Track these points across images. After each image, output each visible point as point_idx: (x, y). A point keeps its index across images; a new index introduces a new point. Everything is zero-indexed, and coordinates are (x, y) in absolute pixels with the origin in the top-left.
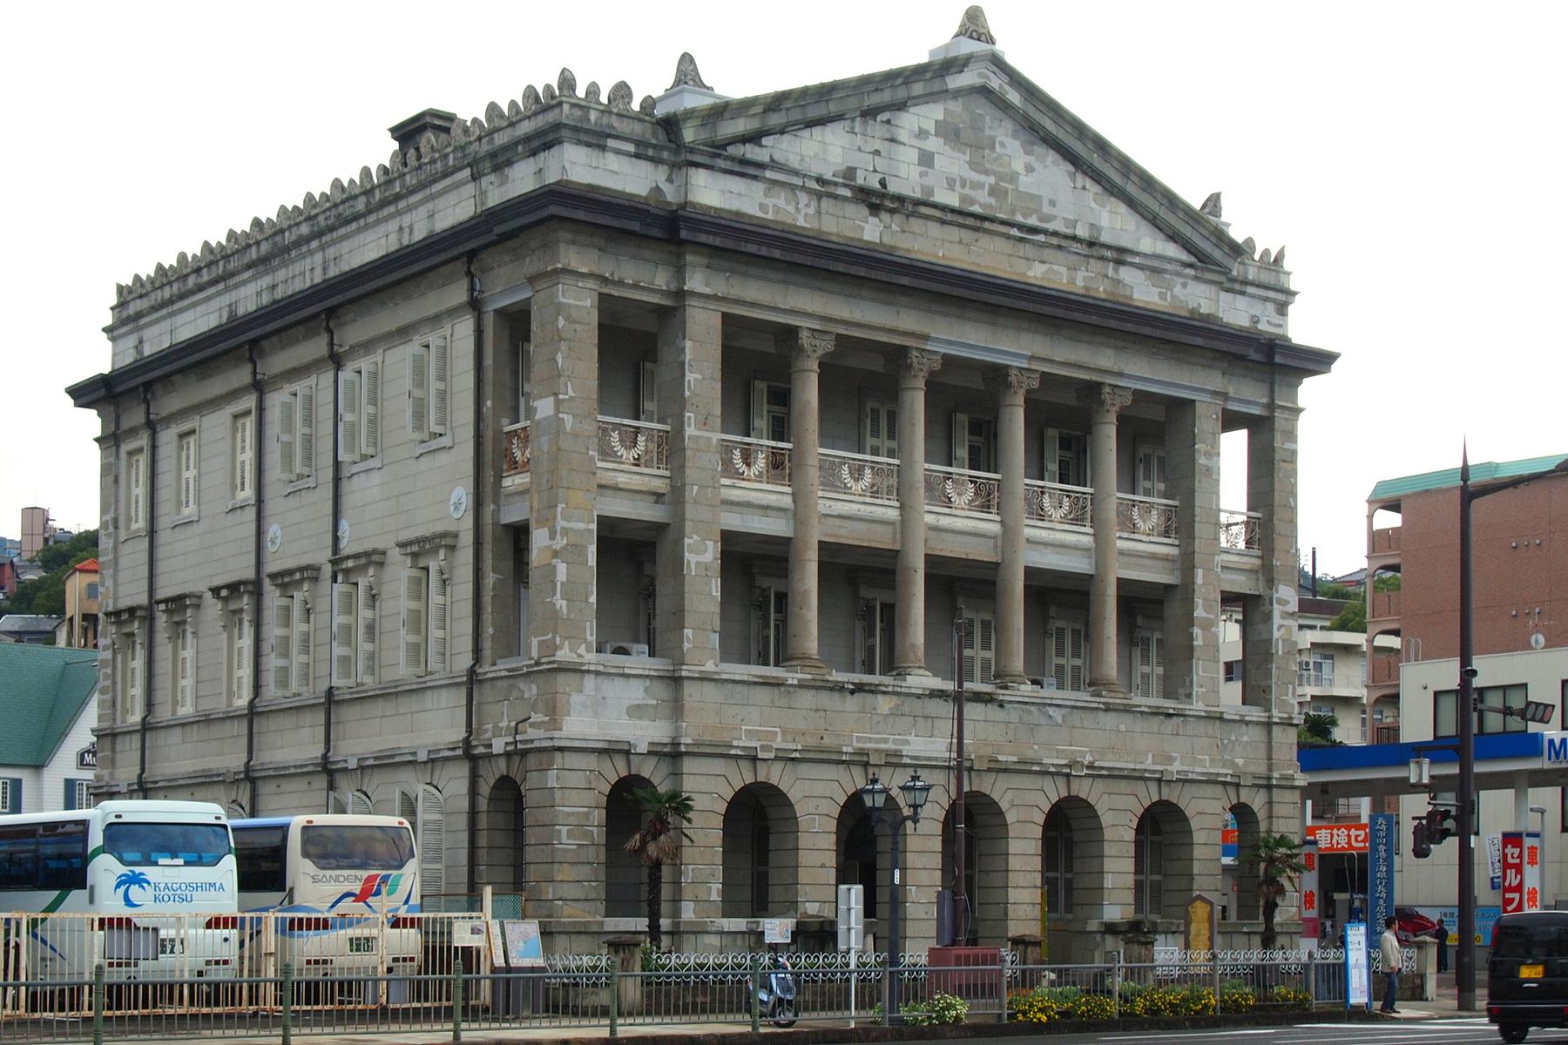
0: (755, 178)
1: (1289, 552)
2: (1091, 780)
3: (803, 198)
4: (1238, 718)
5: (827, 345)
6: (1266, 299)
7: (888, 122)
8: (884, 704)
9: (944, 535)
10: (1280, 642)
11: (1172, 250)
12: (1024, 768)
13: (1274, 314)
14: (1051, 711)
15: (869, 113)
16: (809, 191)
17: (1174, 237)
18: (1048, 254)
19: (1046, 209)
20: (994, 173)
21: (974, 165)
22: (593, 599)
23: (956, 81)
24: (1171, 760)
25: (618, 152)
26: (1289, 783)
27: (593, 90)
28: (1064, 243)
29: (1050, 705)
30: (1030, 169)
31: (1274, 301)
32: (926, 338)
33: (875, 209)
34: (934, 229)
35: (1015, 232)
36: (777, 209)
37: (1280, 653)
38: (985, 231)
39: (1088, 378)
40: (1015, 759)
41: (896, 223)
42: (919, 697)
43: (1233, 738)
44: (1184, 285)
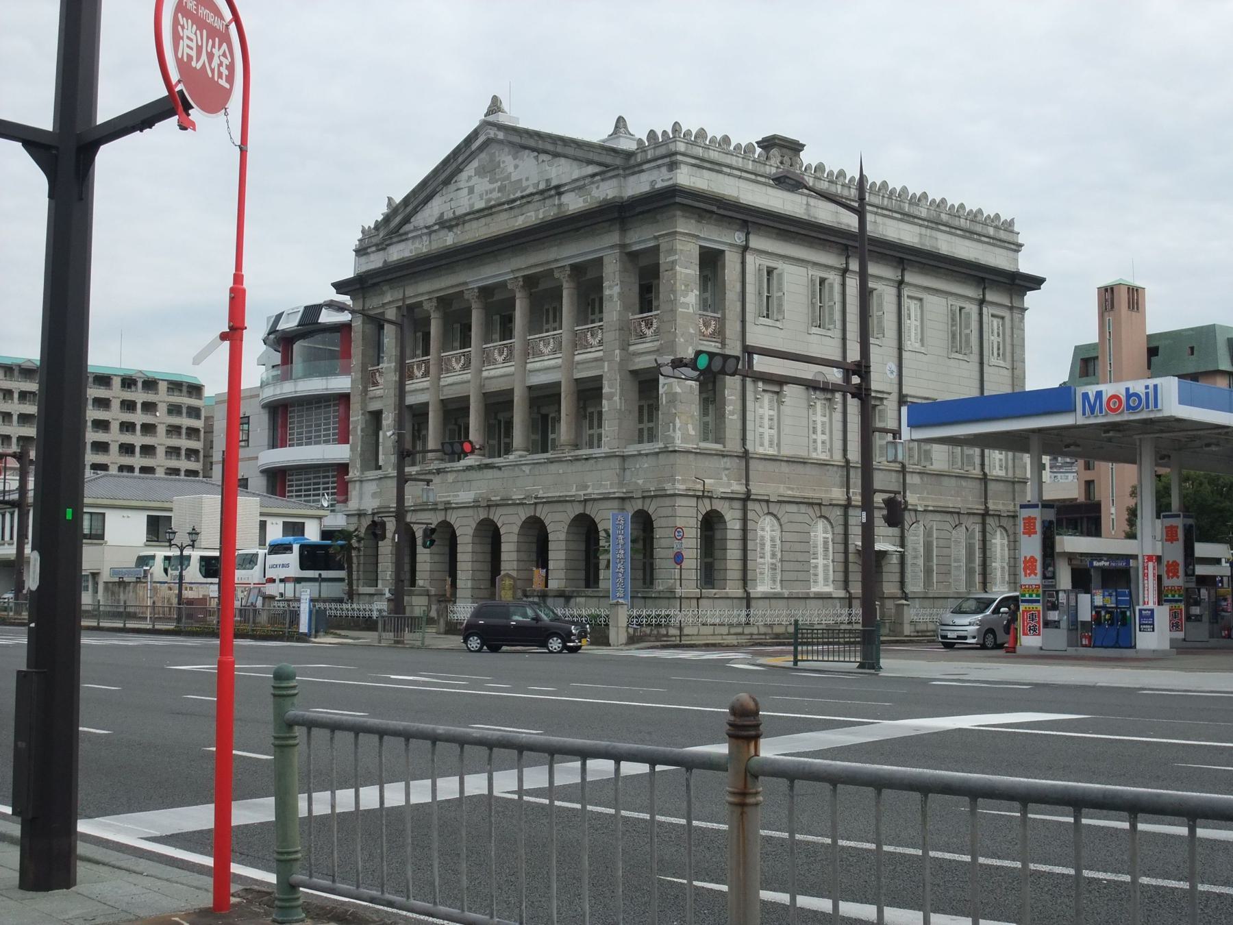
0: (407, 239)
1: (670, 332)
2: (541, 505)
3: (425, 238)
4: (636, 453)
5: (434, 303)
6: (659, 167)
7: (456, 181)
8: (450, 478)
9: (494, 380)
10: (664, 396)
11: (591, 169)
12: (504, 503)
13: (666, 172)
14: (524, 468)
15: (447, 182)
16: (425, 234)
17: (590, 162)
18: (525, 209)
19: (525, 184)
20: (499, 179)
21: (491, 182)
22: (359, 449)
23: (475, 146)
24: (586, 487)
25: (373, 252)
26: (663, 493)
27: (369, 227)
28: (529, 199)
29: (522, 464)
30: (516, 167)
31: (664, 165)
32: (466, 283)
33: (450, 228)
34: (475, 224)
35: (506, 206)
36: (416, 248)
37: (664, 402)
38: (495, 213)
39: (542, 269)
40: (499, 498)
41: (458, 230)
42: (464, 471)
43: (638, 466)
44: (598, 188)
